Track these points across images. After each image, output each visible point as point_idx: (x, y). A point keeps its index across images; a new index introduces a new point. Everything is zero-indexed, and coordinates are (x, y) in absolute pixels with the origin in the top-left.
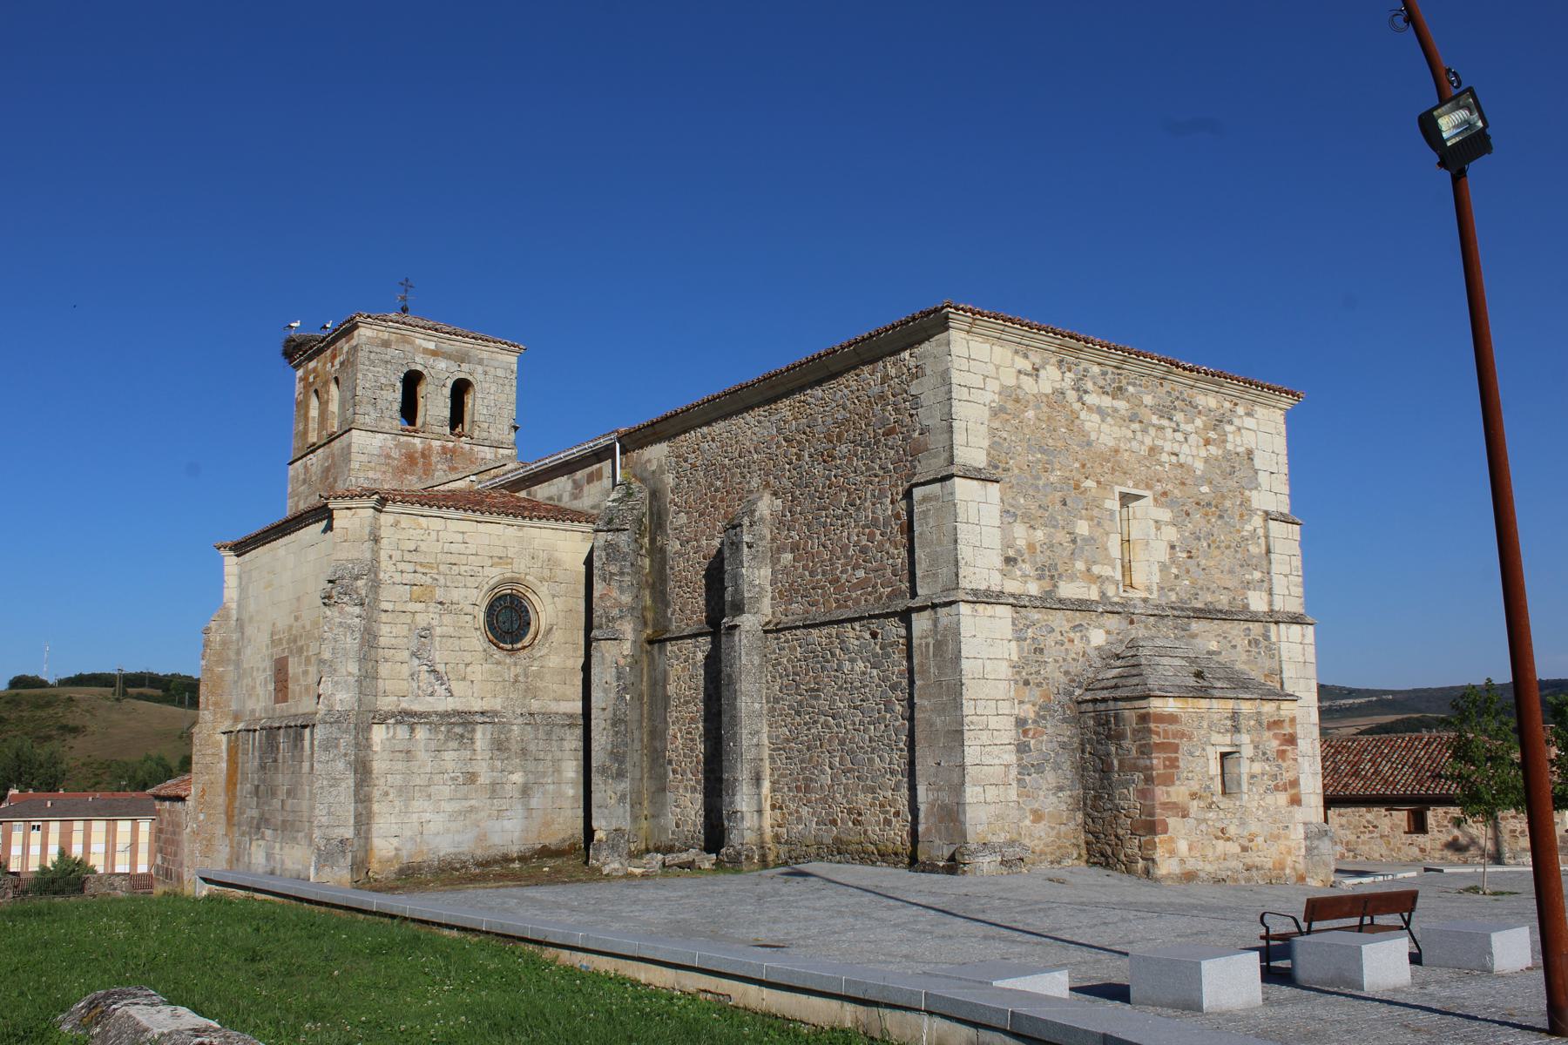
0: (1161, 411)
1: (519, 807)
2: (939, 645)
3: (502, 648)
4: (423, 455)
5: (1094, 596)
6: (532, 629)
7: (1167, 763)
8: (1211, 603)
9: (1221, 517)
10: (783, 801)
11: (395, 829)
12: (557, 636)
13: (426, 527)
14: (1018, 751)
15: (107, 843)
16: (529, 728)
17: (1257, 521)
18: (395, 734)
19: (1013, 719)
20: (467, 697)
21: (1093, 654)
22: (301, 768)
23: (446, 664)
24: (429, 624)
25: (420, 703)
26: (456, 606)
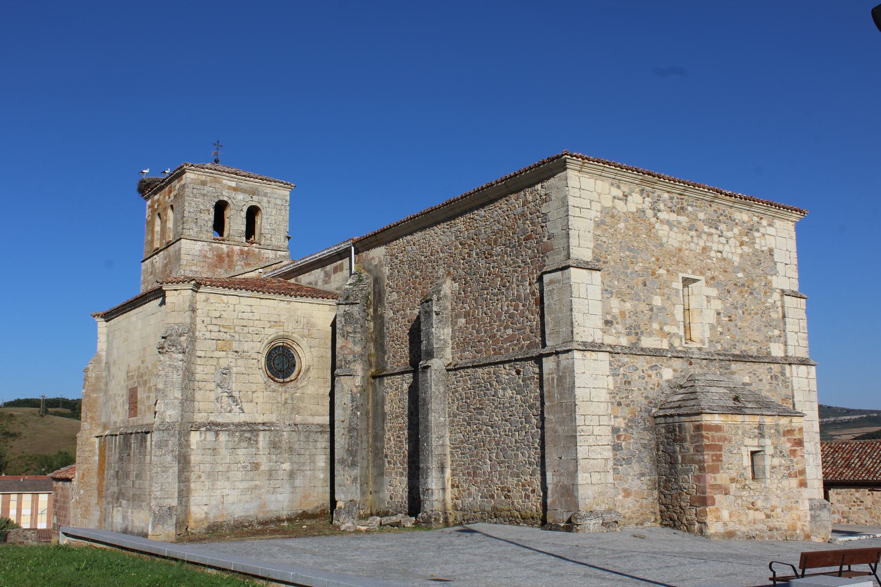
0: (710, 223)
1: (288, 485)
2: (560, 379)
3: (276, 381)
4: (228, 256)
5: (665, 345)
6: (297, 369)
7: (714, 458)
8: (745, 351)
9: (751, 293)
10: (459, 482)
11: (205, 500)
12: (313, 373)
13: (226, 301)
14: (614, 449)
15: (32, 508)
16: (294, 434)
17: (776, 296)
18: (205, 437)
19: (610, 428)
20: (253, 413)
21: (665, 385)
22: (145, 460)
23: (240, 391)
24: (229, 365)
25: (222, 417)
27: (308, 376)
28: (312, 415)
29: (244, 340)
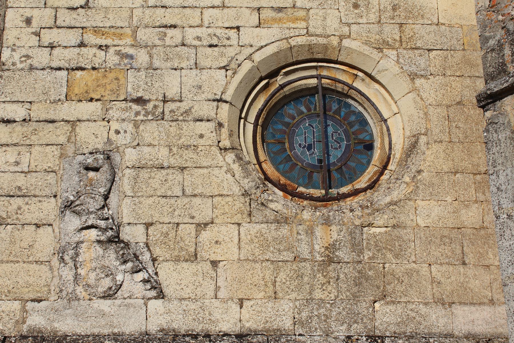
3: (302, 196)
6: (377, 154)
23: (148, 225)
27: (414, 169)
28: (441, 302)
29: (169, 65)
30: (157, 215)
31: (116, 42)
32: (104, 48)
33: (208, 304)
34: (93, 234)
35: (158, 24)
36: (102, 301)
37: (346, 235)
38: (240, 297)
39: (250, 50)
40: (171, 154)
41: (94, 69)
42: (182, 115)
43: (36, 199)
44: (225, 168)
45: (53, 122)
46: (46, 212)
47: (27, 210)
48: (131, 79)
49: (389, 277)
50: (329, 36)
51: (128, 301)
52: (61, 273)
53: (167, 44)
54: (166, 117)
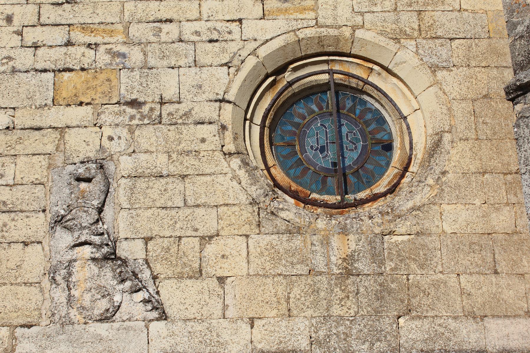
3: (315, 203)
6: (397, 155)
23: (147, 240)
26: (168, 108)
27: (438, 170)
29: (165, 63)
30: (157, 228)
31: (106, 40)
32: (93, 46)
33: (215, 325)
34: (87, 250)
35: (152, 19)
36: (99, 324)
37: (365, 244)
38: (251, 316)
39: (254, 45)
40: (171, 161)
41: (83, 69)
42: (181, 118)
43: (23, 214)
44: (230, 175)
45: (39, 129)
46: (34, 229)
47: (13, 227)
48: (124, 80)
49: (414, 290)
50: (340, 27)
51: (127, 323)
52: (53, 295)
53: (163, 40)
54: (163, 121)
